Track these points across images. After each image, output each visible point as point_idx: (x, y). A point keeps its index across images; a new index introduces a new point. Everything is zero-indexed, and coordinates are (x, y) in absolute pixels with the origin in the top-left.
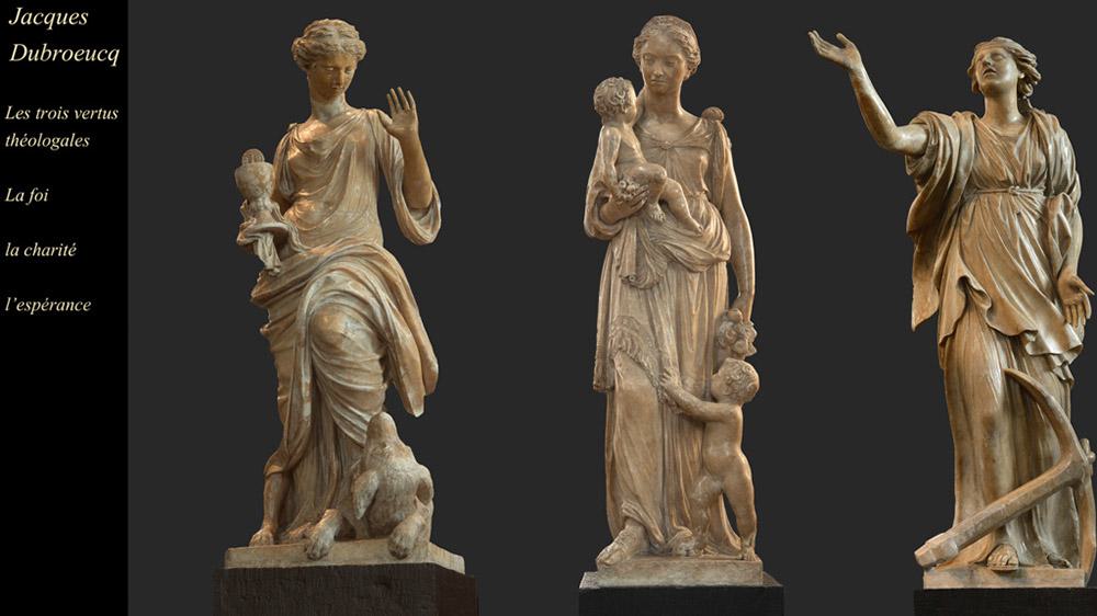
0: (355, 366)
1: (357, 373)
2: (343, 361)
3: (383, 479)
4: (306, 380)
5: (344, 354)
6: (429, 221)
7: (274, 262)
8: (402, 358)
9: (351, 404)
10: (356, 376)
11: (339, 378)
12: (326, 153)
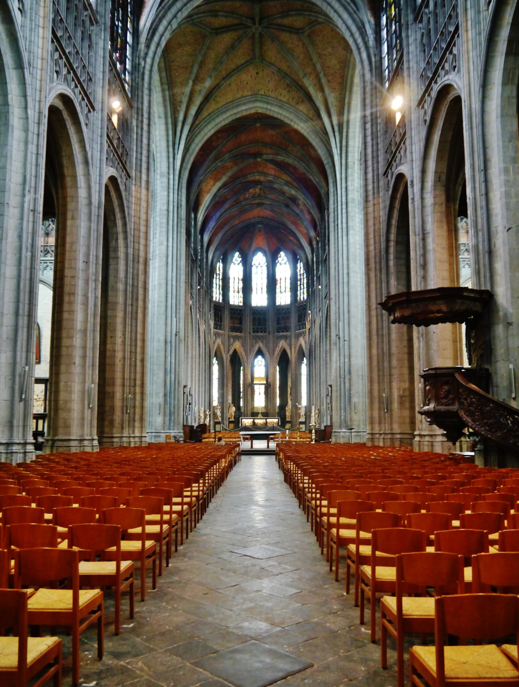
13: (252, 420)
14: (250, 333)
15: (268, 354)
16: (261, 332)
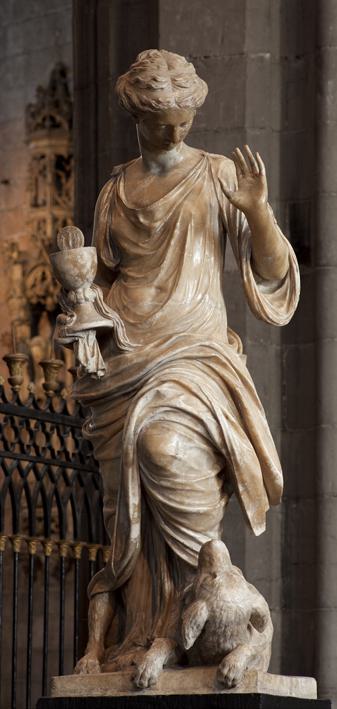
0: (188, 488)
1: (189, 494)
2: (174, 483)
3: (212, 611)
4: (134, 500)
5: (175, 476)
7: (97, 365)
8: (240, 474)
9: (181, 524)
10: (188, 497)
11: (170, 500)
12: (158, 225)
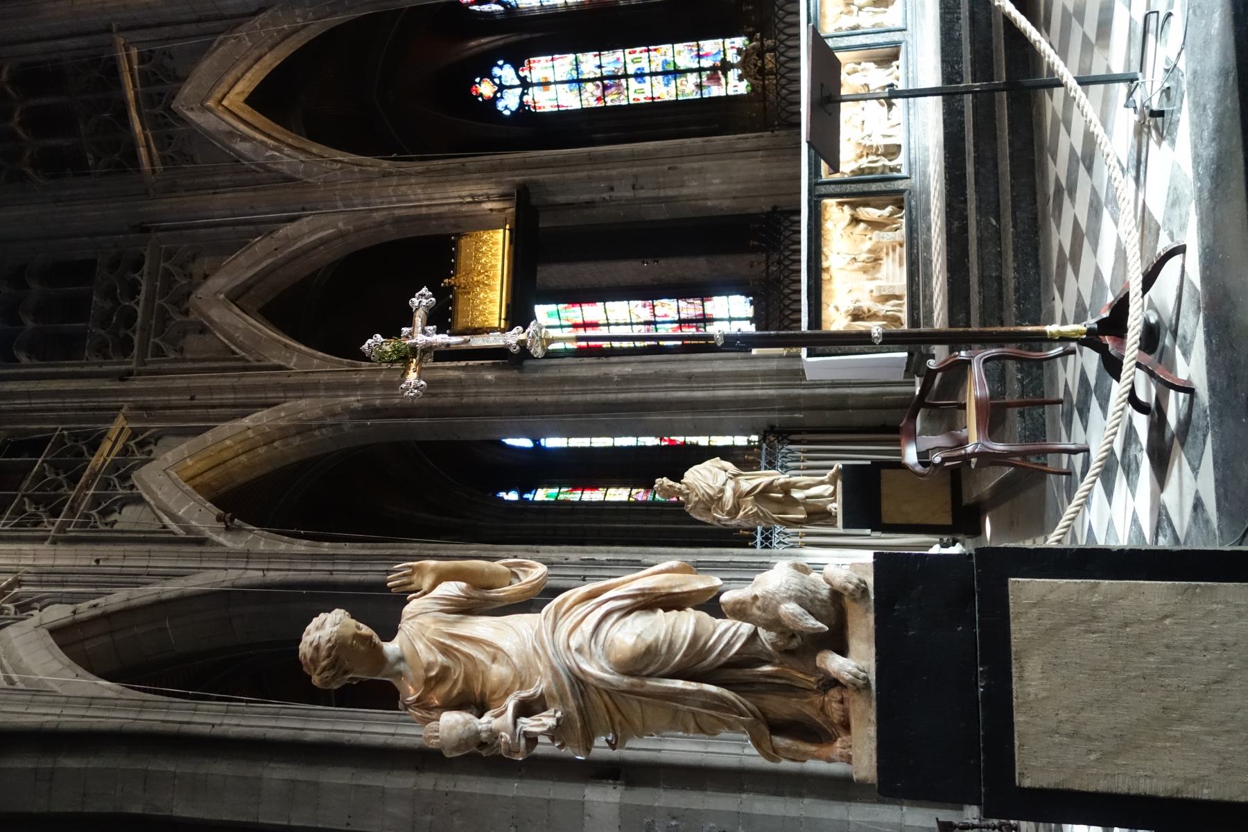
0: (670, 630)
1: (676, 630)
2: (664, 641)
3: (790, 598)
4: (679, 684)
5: (657, 639)
6: (524, 571)
7: (550, 716)
8: (663, 588)
9: (706, 643)
10: (680, 631)
11: (680, 649)
12: (441, 658)
13: (836, 215)
14: (124, 376)
15: (288, 229)
16: (134, 290)
